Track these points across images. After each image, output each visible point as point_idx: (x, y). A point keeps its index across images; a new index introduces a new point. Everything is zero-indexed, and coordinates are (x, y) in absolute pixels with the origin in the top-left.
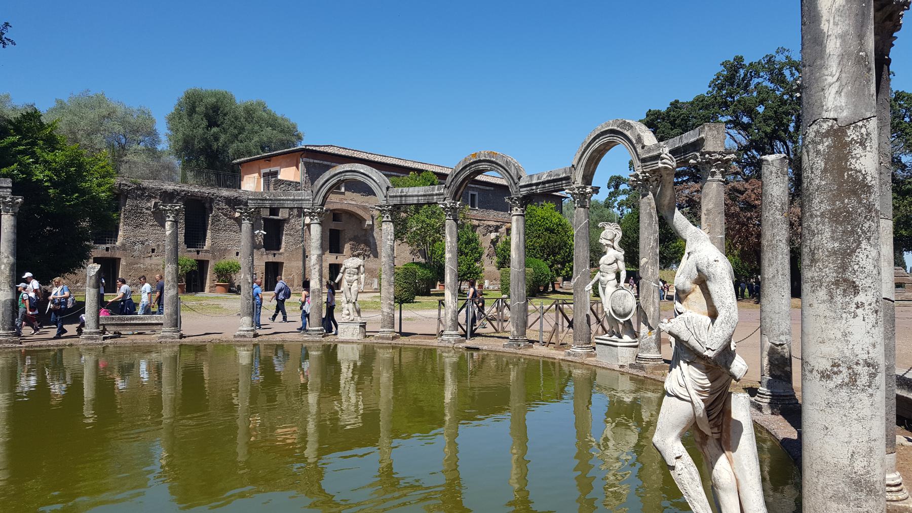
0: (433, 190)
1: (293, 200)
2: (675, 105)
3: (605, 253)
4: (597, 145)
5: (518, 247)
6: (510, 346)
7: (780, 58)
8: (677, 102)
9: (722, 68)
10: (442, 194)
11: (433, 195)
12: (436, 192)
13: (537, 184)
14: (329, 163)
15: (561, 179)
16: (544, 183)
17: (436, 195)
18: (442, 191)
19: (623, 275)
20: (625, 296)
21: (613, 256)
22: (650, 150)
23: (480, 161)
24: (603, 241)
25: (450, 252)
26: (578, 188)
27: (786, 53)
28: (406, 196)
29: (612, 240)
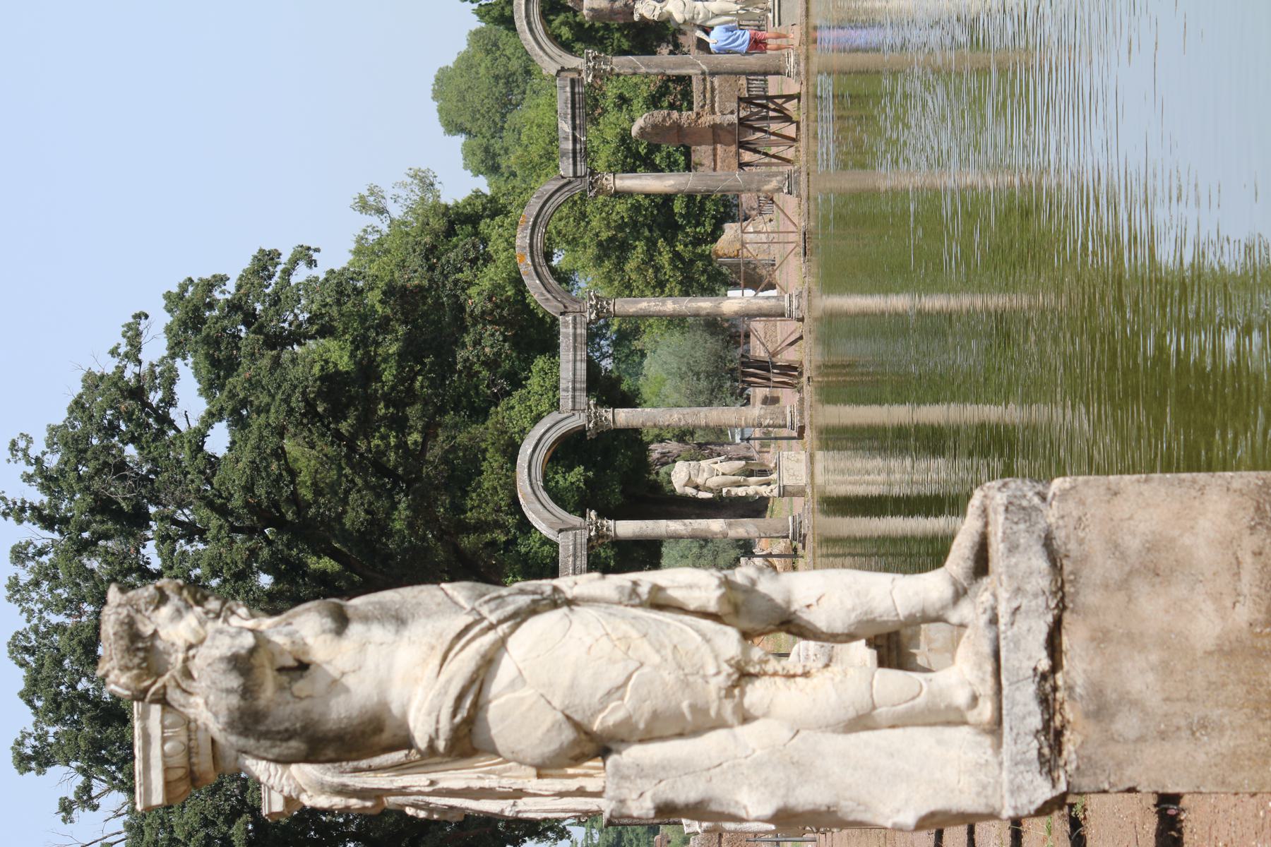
0: (567, 336)
3: (670, 14)
4: (540, 27)
6: (797, 183)
10: (575, 319)
11: (575, 335)
12: (571, 330)
15: (573, 93)
16: (574, 128)
17: (575, 328)
18: (570, 318)
23: (531, 246)
24: (657, 13)
25: (664, 303)
26: (588, 60)
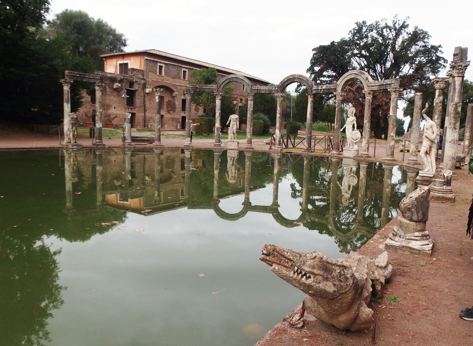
1: (209, 89)
2: (333, 43)
5: (310, 114)
7: (382, 24)
8: (334, 42)
9: (356, 25)
13: (321, 90)
14: (157, 60)
19: (356, 126)
20: (357, 133)
21: (351, 120)
22: (371, 83)
27: (386, 21)
28: (260, 90)
29: (352, 113)
